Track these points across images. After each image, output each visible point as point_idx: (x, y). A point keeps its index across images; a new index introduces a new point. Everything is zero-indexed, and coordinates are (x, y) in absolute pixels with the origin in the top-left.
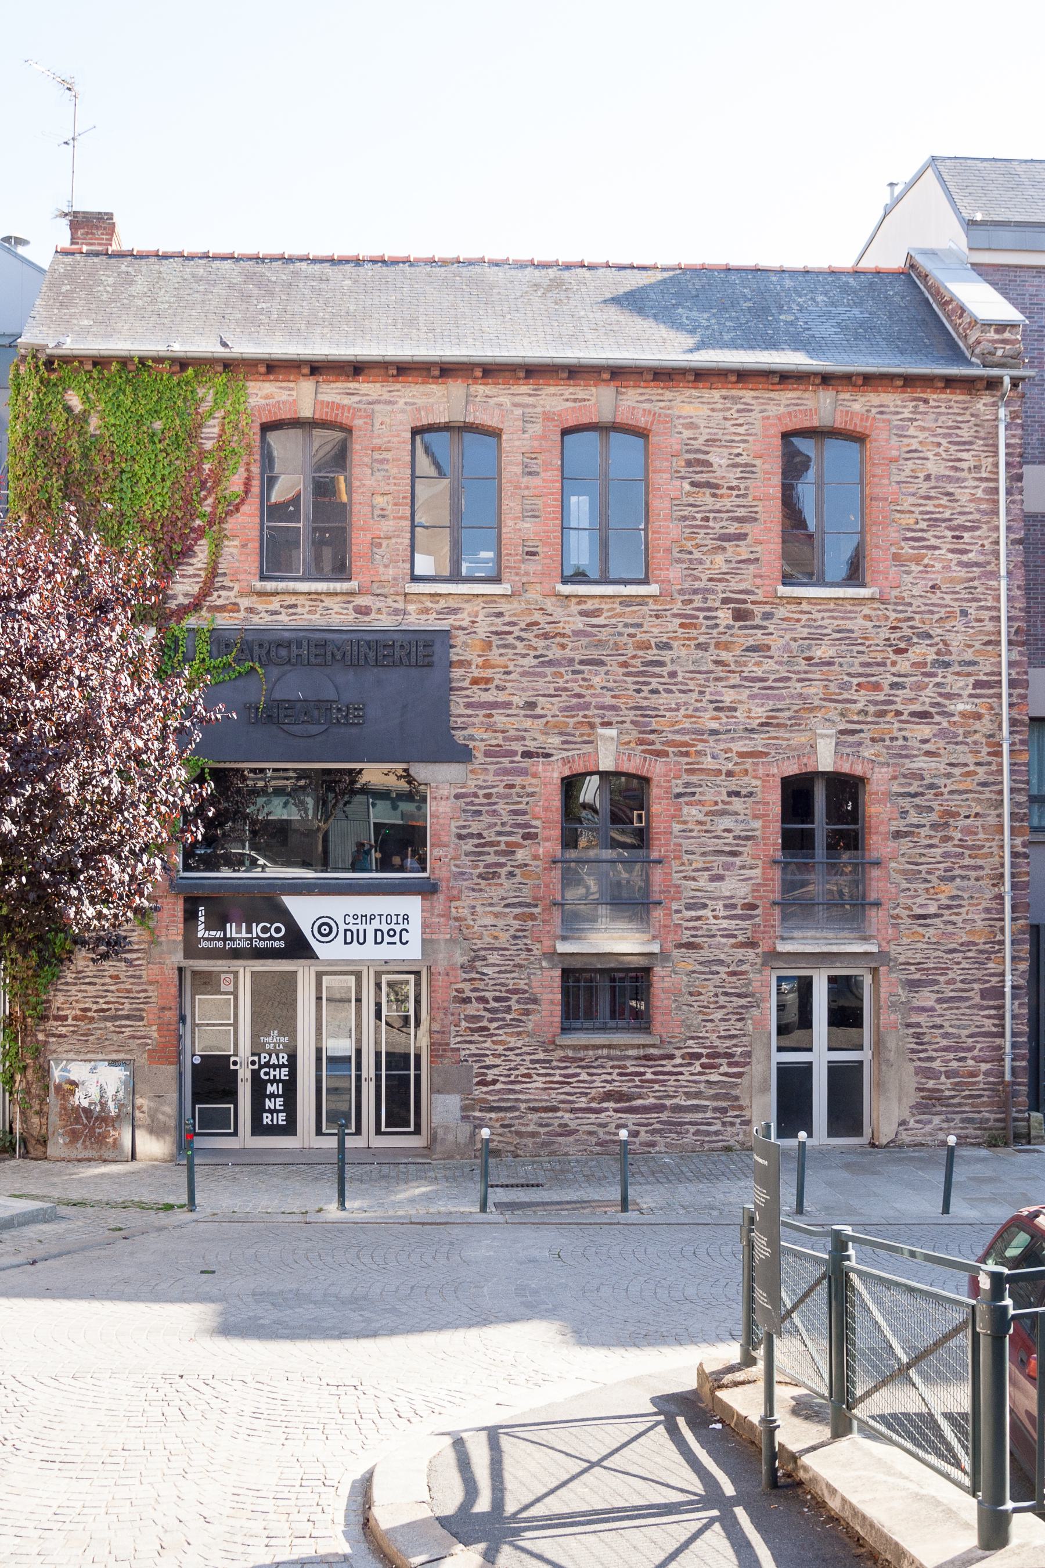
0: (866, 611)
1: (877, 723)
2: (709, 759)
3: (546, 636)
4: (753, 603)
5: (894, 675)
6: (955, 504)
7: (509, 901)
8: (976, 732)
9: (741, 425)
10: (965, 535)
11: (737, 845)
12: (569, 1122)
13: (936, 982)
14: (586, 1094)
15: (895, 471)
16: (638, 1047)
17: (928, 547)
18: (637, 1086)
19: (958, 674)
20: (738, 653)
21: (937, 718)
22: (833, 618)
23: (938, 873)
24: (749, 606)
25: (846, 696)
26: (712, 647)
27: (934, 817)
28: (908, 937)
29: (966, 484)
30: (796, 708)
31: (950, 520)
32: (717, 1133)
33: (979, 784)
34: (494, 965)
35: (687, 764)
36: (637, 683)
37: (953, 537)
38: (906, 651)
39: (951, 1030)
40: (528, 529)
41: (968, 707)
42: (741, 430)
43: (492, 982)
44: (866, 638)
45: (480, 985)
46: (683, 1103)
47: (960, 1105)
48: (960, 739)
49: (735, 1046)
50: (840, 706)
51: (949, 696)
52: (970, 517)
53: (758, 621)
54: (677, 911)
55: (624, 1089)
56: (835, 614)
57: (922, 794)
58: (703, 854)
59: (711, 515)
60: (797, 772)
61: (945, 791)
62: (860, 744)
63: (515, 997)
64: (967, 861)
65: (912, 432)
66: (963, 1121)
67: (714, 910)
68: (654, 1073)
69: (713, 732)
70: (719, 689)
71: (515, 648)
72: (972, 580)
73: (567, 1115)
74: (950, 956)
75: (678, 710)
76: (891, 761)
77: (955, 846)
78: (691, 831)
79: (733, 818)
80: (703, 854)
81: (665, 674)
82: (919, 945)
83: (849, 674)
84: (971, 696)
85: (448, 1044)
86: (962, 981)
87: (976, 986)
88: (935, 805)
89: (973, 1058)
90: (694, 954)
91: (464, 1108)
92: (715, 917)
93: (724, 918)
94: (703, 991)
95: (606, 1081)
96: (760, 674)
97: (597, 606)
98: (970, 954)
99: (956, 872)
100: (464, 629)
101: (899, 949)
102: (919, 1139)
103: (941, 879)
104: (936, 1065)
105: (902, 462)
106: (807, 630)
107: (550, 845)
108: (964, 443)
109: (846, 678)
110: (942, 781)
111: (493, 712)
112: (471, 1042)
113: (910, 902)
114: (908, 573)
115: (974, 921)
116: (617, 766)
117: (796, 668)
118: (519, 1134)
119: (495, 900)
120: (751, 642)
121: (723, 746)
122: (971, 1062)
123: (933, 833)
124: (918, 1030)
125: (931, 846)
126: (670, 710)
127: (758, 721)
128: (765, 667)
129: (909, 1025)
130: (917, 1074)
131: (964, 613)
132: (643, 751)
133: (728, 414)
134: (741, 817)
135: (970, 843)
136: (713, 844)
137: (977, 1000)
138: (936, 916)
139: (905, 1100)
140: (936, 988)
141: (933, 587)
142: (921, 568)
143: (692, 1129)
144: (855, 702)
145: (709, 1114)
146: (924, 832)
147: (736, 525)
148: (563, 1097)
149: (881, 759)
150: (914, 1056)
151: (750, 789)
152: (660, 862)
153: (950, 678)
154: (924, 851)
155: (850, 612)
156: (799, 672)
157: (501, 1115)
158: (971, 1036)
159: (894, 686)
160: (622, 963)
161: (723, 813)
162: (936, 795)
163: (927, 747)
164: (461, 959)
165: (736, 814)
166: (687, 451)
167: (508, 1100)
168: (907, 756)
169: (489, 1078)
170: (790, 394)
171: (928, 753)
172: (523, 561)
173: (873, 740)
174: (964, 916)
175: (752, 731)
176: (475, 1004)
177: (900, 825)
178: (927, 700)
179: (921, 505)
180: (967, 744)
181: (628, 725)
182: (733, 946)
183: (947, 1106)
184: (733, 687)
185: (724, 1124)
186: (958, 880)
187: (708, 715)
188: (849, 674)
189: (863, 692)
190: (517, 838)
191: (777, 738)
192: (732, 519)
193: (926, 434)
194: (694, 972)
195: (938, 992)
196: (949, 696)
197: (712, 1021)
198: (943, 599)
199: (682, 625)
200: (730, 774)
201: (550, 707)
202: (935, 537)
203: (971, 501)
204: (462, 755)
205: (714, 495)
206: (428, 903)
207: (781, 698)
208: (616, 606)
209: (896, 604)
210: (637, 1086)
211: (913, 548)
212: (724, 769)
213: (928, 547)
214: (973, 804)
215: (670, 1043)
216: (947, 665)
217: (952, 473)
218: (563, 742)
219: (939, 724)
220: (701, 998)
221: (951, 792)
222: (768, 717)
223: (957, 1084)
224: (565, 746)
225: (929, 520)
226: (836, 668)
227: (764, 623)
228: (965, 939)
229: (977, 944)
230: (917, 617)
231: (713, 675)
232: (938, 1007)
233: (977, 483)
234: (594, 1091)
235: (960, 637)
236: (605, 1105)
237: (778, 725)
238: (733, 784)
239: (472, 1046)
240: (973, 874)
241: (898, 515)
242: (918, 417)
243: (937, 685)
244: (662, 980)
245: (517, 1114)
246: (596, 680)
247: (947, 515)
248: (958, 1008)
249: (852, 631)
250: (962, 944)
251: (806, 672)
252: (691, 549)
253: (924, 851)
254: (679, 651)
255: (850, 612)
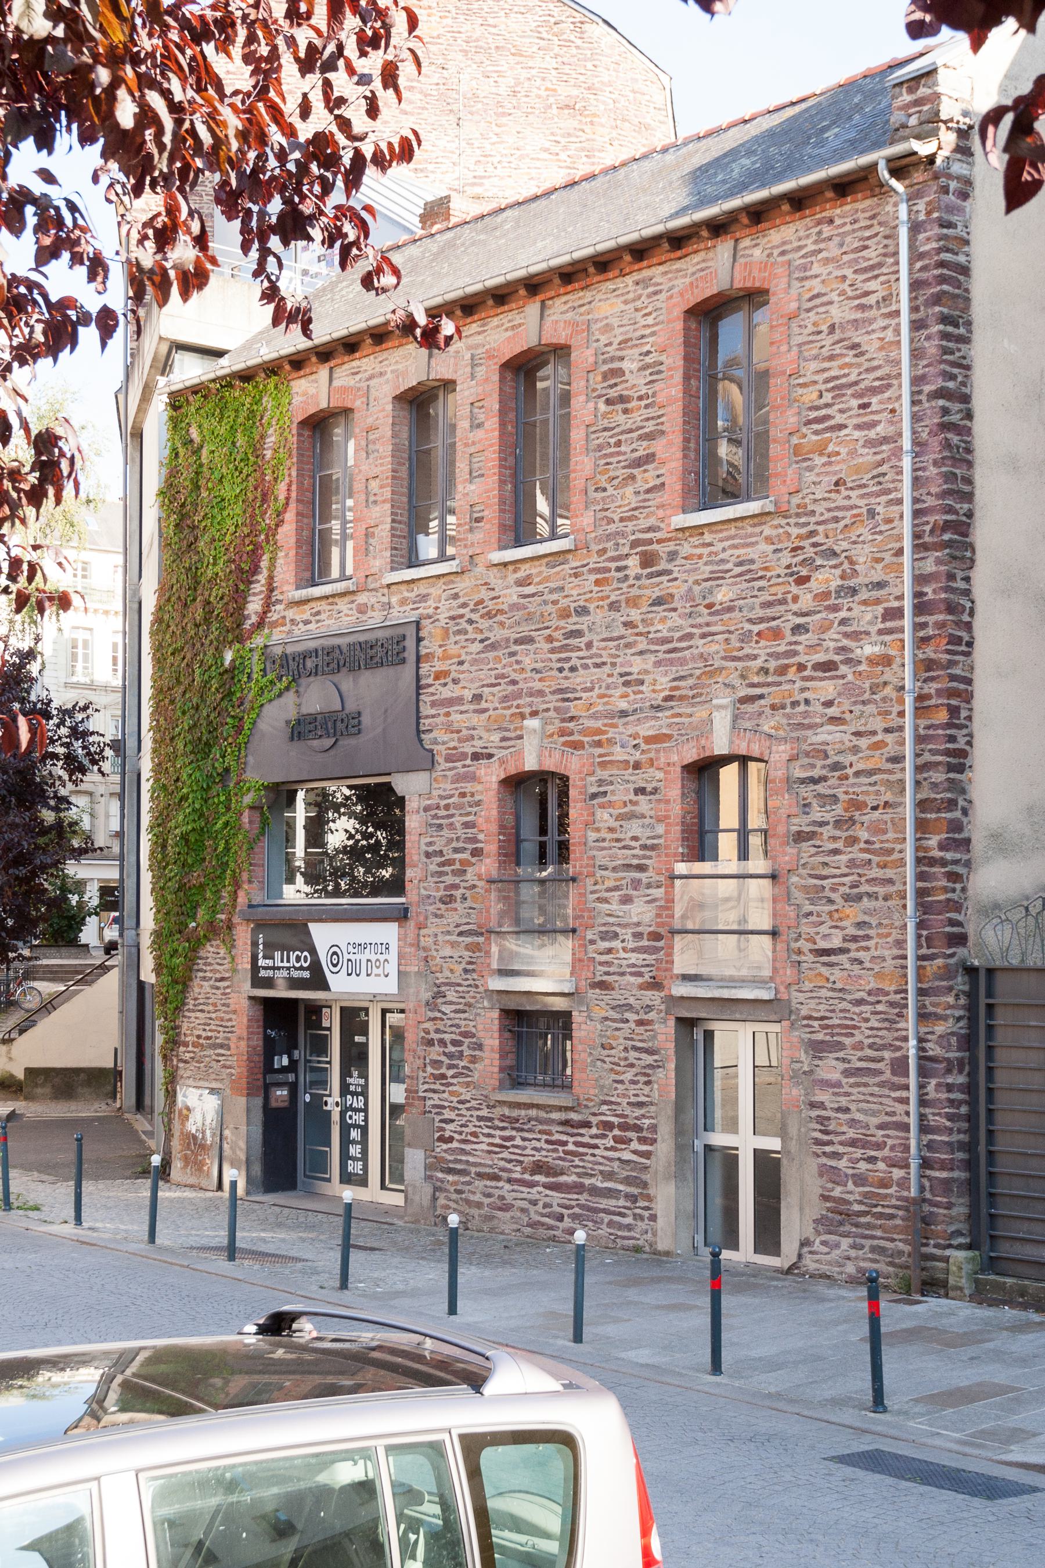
0: (768, 531)
1: (779, 684)
2: (619, 749)
3: (489, 615)
4: (659, 541)
5: (795, 614)
6: (862, 359)
7: (461, 929)
8: (885, 683)
9: (650, 314)
10: (874, 400)
11: (645, 857)
12: (506, 1195)
13: (840, 1046)
14: (521, 1162)
15: (796, 330)
16: (560, 1109)
17: (832, 428)
18: (560, 1158)
19: (865, 603)
20: (644, 609)
21: (843, 669)
22: (734, 547)
23: (842, 889)
24: (655, 546)
25: (747, 651)
26: (623, 605)
27: (839, 810)
28: (811, 981)
29: (874, 326)
30: (698, 672)
31: (856, 383)
32: (629, 1227)
33: (889, 760)
34: (451, 1003)
35: (600, 756)
36: (559, 660)
37: (861, 407)
38: (807, 579)
39: (859, 1116)
40: (473, 492)
41: (877, 649)
42: (650, 320)
43: (450, 1023)
44: (766, 569)
45: (440, 1025)
46: (599, 1184)
47: (869, 1226)
48: (866, 696)
49: (643, 1116)
50: (740, 665)
51: (856, 636)
52: (879, 373)
53: (663, 565)
54: (592, 942)
55: (549, 1159)
56: (736, 541)
57: (824, 779)
58: (615, 869)
59: (623, 437)
60: (695, 757)
61: (850, 771)
62: (760, 714)
63: (467, 1041)
64: (875, 873)
65: (816, 269)
66: (873, 1249)
67: (623, 941)
68: (576, 1144)
69: (624, 714)
70: (628, 658)
71: (466, 632)
72: (880, 463)
73: (508, 1187)
74: (857, 1010)
75: (592, 689)
76: (794, 735)
77: (862, 850)
78: (604, 840)
79: (640, 821)
80: (615, 869)
81: (583, 646)
82: (824, 993)
83: (750, 621)
84: (881, 632)
85: (417, 1092)
86: (870, 1046)
87: (887, 1054)
88: (839, 792)
89: (884, 1160)
90: (607, 997)
91: (427, 1167)
92: (624, 949)
93: (633, 950)
94: (614, 1043)
95: (535, 1149)
96: (665, 634)
97: (528, 572)
98: (880, 1008)
99: (865, 888)
100: (430, 617)
101: (801, 997)
102: (825, 1268)
103: (847, 898)
104: (842, 1164)
105: (804, 315)
106: (709, 568)
107: (489, 866)
108: (872, 268)
109: (748, 626)
110: (846, 759)
111: (451, 709)
112: (434, 1091)
113: (812, 931)
114: (810, 469)
115: (884, 960)
116: (540, 765)
117: (700, 620)
118: (468, 1202)
119: (451, 928)
120: (657, 593)
121: (631, 730)
122: (881, 1165)
123: (838, 833)
124: (823, 1113)
125: (836, 852)
126: (586, 690)
127: (663, 694)
128: (670, 623)
129: (813, 1105)
130: (821, 1175)
131: (872, 513)
132: (564, 744)
133: (639, 304)
134: (647, 821)
135: (877, 846)
136: (623, 856)
137: (888, 1075)
138: (842, 951)
139: (807, 1211)
140: (841, 1054)
141: (837, 484)
142: (825, 459)
143: (607, 1218)
144: (755, 657)
145: (622, 1202)
146: (827, 831)
147: (645, 443)
148: (502, 1163)
149: (781, 733)
150: (818, 1149)
151: (654, 784)
152: (574, 880)
153: (857, 609)
154: (827, 859)
155: (751, 536)
156: (700, 626)
157: (456, 1178)
158: (881, 1127)
159: (797, 629)
160: (545, 1005)
161: (632, 816)
162: (840, 778)
163: (832, 711)
164: (427, 995)
165: (643, 816)
166: (604, 362)
167: (460, 1161)
168: (810, 727)
169: (447, 1134)
170: (696, 258)
171: (834, 720)
172: (471, 530)
173: (773, 707)
174: (874, 953)
175: (658, 708)
176: (437, 1048)
177: (800, 823)
178: (832, 644)
179: (824, 370)
180: (875, 702)
181: (552, 714)
182: (641, 987)
183: (857, 1225)
184: (641, 653)
185: (636, 1216)
186: (865, 899)
187: (618, 692)
188: (750, 621)
189: (763, 643)
190: (466, 856)
191: (679, 715)
192: (640, 438)
193: (830, 267)
194: (606, 1019)
195: (844, 1060)
196: (856, 636)
197: (621, 1082)
198: (849, 497)
199: (597, 583)
200: (637, 766)
201: (492, 698)
202: (841, 411)
203: (881, 348)
204: (429, 763)
205: (626, 411)
206: (402, 930)
207: (683, 662)
208: (543, 568)
209: (798, 515)
210: (560, 1158)
211: (816, 433)
212: (632, 760)
213: (832, 428)
214: (882, 789)
215: (586, 1107)
216: (854, 591)
217: (859, 315)
218: (503, 739)
219: (843, 677)
220: (613, 1052)
221: (857, 774)
222: (672, 689)
223: (866, 1195)
224: (504, 744)
225: (833, 388)
226: (736, 614)
227: (669, 567)
228: (873, 985)
229: (887, 994)
230: (821, 528)
231: (622, 641)
232: (844, 1081)
233: (887, 322)
234: (526, 1159)
235: (867, 548)
236: (537, 1178)
237: (682, 698)
238: (639, 779)
239: (435, 1096)
240: (881, 890)
241: (800, 391)
242: (822, 246)
243: (843, 622)
244: (583, 1028)
245: (467, 1179)
246: (527, 662)
247: (853, 378)
248: (866, 1085)
249: (752, 561)
250: (870, 993)
251: (708, 625)
252: (604, 484)
253: (827, 859)
254: (598, 616)
255: (751, 536)
